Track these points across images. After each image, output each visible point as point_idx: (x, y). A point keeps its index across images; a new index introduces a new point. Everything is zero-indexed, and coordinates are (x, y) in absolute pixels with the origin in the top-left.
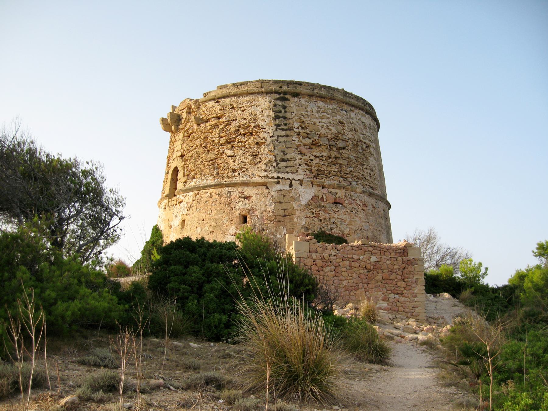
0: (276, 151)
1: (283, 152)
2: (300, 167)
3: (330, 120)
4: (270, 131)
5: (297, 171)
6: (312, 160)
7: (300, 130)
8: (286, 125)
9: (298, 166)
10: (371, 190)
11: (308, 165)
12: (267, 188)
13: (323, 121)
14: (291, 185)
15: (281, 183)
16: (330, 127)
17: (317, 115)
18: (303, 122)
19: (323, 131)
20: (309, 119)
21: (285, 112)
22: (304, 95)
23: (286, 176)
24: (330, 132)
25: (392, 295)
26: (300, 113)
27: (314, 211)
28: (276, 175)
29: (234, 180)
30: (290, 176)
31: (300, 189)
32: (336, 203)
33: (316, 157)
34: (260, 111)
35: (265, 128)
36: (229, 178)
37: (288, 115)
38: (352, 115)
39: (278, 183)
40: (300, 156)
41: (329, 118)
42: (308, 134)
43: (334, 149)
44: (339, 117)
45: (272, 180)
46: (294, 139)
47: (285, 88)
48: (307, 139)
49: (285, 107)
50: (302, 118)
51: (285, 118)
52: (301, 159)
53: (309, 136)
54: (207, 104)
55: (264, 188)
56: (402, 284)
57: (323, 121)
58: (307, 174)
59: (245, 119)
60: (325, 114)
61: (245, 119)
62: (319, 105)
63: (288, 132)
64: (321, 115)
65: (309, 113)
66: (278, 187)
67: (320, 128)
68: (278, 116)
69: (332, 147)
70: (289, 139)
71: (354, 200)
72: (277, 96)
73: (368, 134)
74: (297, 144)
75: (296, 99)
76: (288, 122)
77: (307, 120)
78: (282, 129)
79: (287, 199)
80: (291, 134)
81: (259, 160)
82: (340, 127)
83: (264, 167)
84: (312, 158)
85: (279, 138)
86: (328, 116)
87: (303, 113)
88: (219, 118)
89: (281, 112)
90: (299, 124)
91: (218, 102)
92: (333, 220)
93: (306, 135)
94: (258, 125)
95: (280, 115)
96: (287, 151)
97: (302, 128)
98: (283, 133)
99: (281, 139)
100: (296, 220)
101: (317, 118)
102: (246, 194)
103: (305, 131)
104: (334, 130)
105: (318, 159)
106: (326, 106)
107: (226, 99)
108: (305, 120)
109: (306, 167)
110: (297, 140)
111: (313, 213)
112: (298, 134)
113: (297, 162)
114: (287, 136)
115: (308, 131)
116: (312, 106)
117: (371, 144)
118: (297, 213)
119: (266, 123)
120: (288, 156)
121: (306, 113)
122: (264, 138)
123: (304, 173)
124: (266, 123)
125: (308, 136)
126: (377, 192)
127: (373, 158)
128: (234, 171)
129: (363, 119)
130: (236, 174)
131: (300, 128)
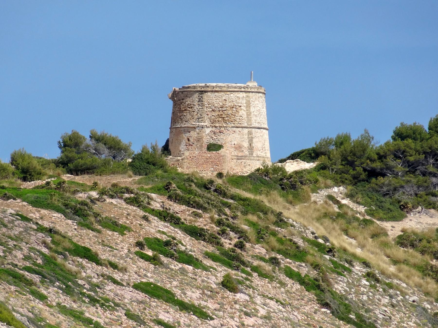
7: (207, 105)
8: (202, 104)
10: (239, 125)
17: (214, 99)
19: (216, 105)
23: (201, 124)
28: (198, 124)
29: (185, 125)
30: (202, 124)
31: (206, 129)
36: (184, 124)
37: (203, 100)
38: (232, 95)
47: (203, 89)
49: (202, 97)
51: (202, 101)
56: (218, 163)
70: (203, 109)
75: (207, 93)
77: (210, 101)
82: (224, 102)
98: (201, 107)
99: (200, 110)
104: (221, 104)
112: (207, 107)
115: (210, 105)
118: (204, 137)
129: (238, 96)
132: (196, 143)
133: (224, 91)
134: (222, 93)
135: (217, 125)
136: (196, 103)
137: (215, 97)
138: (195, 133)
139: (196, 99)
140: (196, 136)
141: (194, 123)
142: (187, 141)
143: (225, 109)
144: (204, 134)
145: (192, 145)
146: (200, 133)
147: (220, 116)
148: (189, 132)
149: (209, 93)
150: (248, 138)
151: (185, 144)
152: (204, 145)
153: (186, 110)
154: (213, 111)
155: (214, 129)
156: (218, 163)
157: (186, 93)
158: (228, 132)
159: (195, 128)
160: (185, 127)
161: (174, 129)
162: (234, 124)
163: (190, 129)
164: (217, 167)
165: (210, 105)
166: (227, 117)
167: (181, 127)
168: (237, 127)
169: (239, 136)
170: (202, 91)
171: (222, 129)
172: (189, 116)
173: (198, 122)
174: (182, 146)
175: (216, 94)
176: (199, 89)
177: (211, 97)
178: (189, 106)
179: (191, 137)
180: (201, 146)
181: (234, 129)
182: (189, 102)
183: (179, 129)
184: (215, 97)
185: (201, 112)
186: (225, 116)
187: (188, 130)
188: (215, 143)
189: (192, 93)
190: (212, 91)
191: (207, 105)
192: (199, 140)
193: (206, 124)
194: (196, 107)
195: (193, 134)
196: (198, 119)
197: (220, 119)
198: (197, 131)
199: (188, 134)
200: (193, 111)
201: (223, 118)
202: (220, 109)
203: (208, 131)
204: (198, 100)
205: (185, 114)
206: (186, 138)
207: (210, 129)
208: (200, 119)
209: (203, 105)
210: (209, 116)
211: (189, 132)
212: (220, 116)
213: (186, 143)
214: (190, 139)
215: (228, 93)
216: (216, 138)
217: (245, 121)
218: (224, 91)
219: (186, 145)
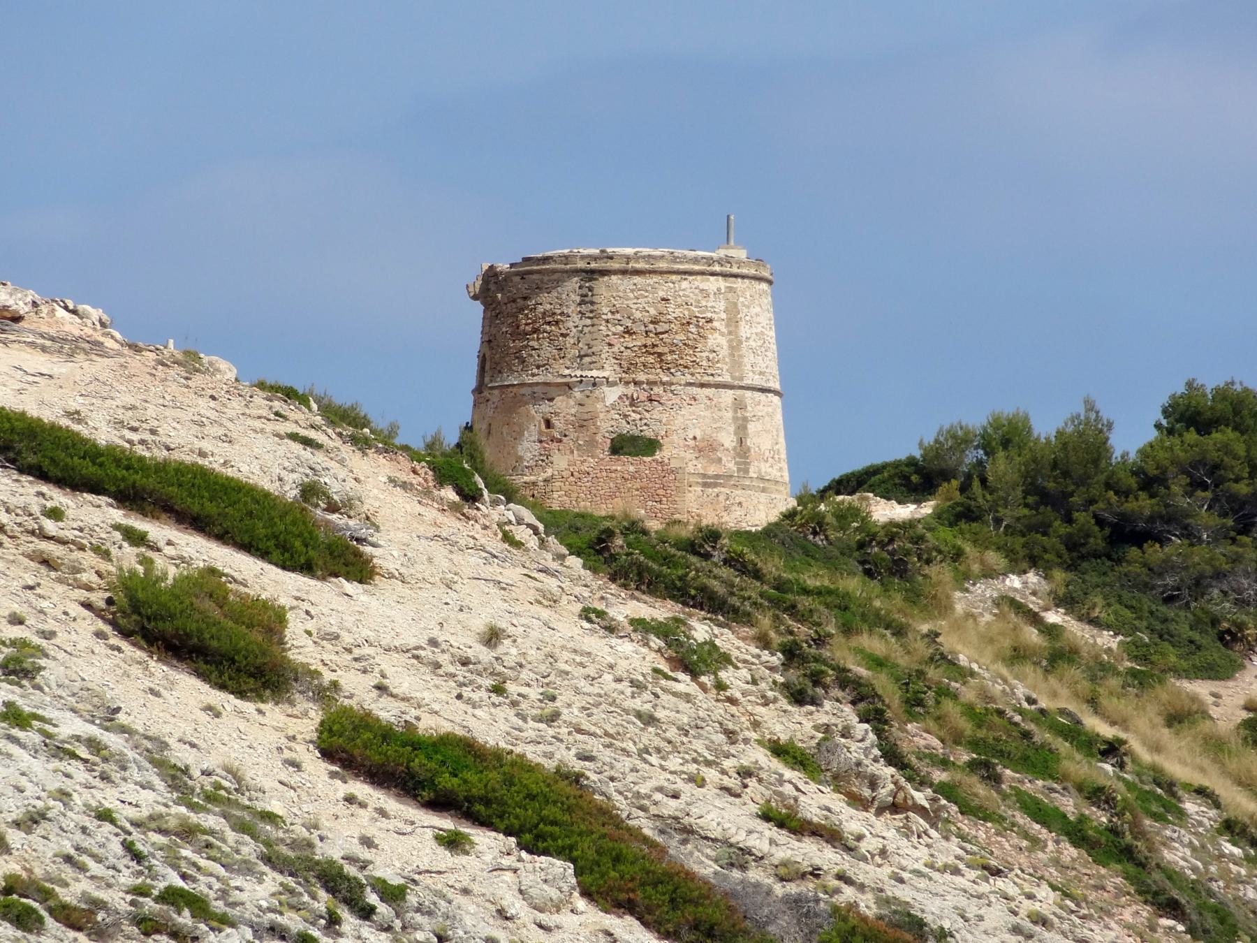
7: (610, 316)
8: (592, 311)
10: (706, 379)
12: (570, 388)
17: (631, 295)
19: (638, 315)
22: (615, 272)
23: (589, 374)
25: (650, 503)
28: (579, 373)
29: (536, 379)
30: (595, 373)
36: (533, 375)
37: (596, 299)
38: (685, 284)
40: (606, 348)
44: (661, 294)
47: (593, 265)
49: (590, 289)
51: (592, 303)
56: (661, 492)
65: (621, 294)
66: (582, 387)
73: (709, 304)
75: (606, 278)
76: (595, 307)
82: (661, 306)
88: (525, 298)
89: (586, 296)
97: (613, 313)
98: (589, 322)
104: (653, 312)
112: (607, 321)
117: (714, 315)
118: (601, 416)
120: (593, 350)
126: (720, 379)
127: (717, 335)
133: (662, 273)
134: (656, 278)
135: (641, 377)
136: (572, 309)
137: (632, 291)
138: (572, 402)
139: (573, 296)
140: (573, 411)
141: (567, 372)
142: (543, 427)
143: (666, 327)
144: (599, 406)
145: (560, 441)
147: (648, 349)
148: (551, 400)
149: (614, 278)
150: (735, 419)
152: (599, 438)
153: (536, 331)
154: (628, 332)
156: (661, 492)
158: (676, 400)
159: (569, 386)
160: (537, 384)
161: (496, 392)
162: (692, 375)
163: (552, 391)
164: (659, 506)
165: (618, 316)
166: (672, 352)
167: (522, 385)
168: (702, 385)
169: (708, 413)
170: (593, 272)
171: (658, 390)
172: (547, 350)
173: (581, 367)
174: (526, 444)
175: (637, 279)
176: (581, 265)
177: (622, 288)
178: (548, 319)
179: (557, 414)
180: (592, 443)
181: (695, 390)
183: (515, 390)
184: (632, 291)
186: (666, 350)
187: (547, 392)
188: (637, 433)
189: (556, 276)
190: (624, 272)
191: (610, 316)
192: (583, 423)
193: (606, 374)
194: (574, 322)
195: (565, 406)
197: (651, 359)
199: (545, 407)
200: (562, 335)
201: (660, 355)
202: (651, 327)
203: (612, 395)
204: (578, 299)
205: (534, 344)
206: (539, 417)
207: (619, 390)
208: (587, 360)
209: (595, 315)
210: (615, 349)
211: (551, 400)
212: (648, 349)
213: (540, 433)
214: (554, 421)
215: (674, 277)
216: (638, 416)
217: (726, 367)
218: (662, 273)
219: (541, 442)
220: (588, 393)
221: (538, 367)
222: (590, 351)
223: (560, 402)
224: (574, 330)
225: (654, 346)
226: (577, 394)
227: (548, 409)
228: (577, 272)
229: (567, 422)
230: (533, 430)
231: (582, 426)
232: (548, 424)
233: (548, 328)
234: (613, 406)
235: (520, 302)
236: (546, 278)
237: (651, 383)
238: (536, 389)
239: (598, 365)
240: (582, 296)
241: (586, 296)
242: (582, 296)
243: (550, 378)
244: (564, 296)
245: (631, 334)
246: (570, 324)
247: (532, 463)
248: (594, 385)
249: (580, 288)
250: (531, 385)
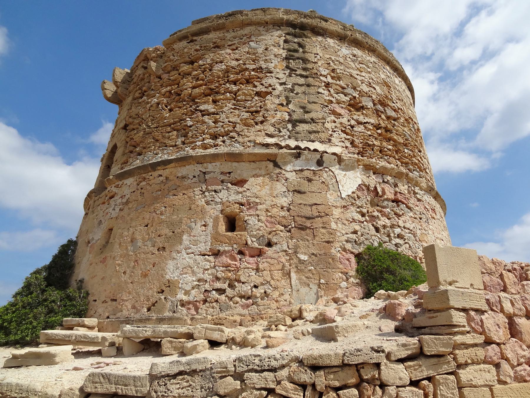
0: (290, 106)
1: (303, 108)
2: (335, 135)
3: (373, 77)
4: (281, 76)
5: (330, 140)
6: (352, 127)
7: (329, 79)
8: (305, 69)
9: (330, 132)
11: (347, 134)
12: (276, 165)
13: (363, 74)
14: (320, 163)
15: (303, 157)
16: (374, 86)
18: (333, 70)
19: (365, 88)
20: (342, 68)
21: (304, 52)
22: (332, 35)
23: (312, 146)
24: (374, 91)
26: (328, 56)
27: (365, 211)
28: (293, 143)
29: (212, 151)
32: (396, 201)
33: (359, 123)
34: (263, 47)
35: (271, 72)
39: (298, 156)
41: (370, 73)
42: (343, 88)
43: (383, 116)
45: (285, 150)
46: (321, 90)
48: (342, 96)
50: (332, 64)
51: (305, 61)
52: (335, 122)
53: (345, 91)
54: (175, 46)
55: (271, 165)
57: (363, 74)
58: (347, 147)
59: (237, 60)
60: (364, 66)
61: (237, 60)
62: (355, 52)
63: (310, 80)
64: (358, 66)
65: (342, 60)
66: (298, 164)
67: (360, 82)
68: (293, 56)
69: (380, 114)
70: (312, 90)
71: (419, 200)
72: (291, 30)
74: (328, 98)
75: (320, 38)
76: (309, 66)
77: (340, 69)
78: (302, 76)
79: (315, 186)
80: (317, 84)
81: (261, 119)
83: (271, 130)
84: (353, 122)
85: (296, 87)
86: (369, 70)
87: (333, 58)
88: (192, 63)
89: (296, 51)
90: (327, 71)
91: (192, 41)
92: (398, 231)
93: (340, 89)
94: (261, 68)
95: (296, 55)
96: (310, 107)
97: (333, 78)
98: (302, 81)
99: (297, 89)
100: (333, 226)
101: (353, 68)
102: (235, 176)
103: (338, 82)
105: (362, 127)
106: (364, 56)
107: (205, 36)
108: (336, 67)
109: (343, 135)
110: (326, 92)
111: (363, 215)
112: (327, 85)
113: (328, 125)
114: (308, 86)
116: (345, 51)
118: (336, 213)
119: (273, 65)
120: (313, 115)
121: (337, 59)
122: (270, 85)
123: (342, 144)
124: (273, 65)
125: (342, 90)
128: (215, 137)
130: (219, 141)
131: (329, 76)
132: (283, 241)
136: (276, 65)
138: (280, 187)
140: (284, 201)
142: (222, 227)
144: (331, 197)
145: (260, 253)
146: (305, 186)
148: (241, 183)
149: (331, 41)
151: (204, 247)
153: (212, 92)
155: (373, 180)
157: (212, 36)
160: (215, 157)
161: (130, 181)
163: (241, 170)
170: (303, 27)
175: (358, 52)
178: (232, 77)
179: (250, 205)
180: (324, 260)
182: (234, 63)
183: (166, 172)
185: (304, 100)
187: (234, 169)
189: (247, 30)
190: (342, 38)
191: (329, 79)
192: (304, 223)
193: (338, 150)
194: (278, 77)
195: (268, 195)
196: (295, 123)
198: (292, 176)
199: (229, 195)
200: (258, 94)
202: (379, 107)
203: (350, 181)
204: (284, 53)
205: (210, 108)
206: (214, 211)
208: (302, 127)
209: (310, 75)
213: (216, 238)
214: (247, 215)
216: (388, 223)
219: (217, 254)
220: (307, 174)
221: (215, 137)
222: (307, 116)
223: (258, 187)
224: (280, 88)
225: (387, 130)
226: (290, 171)
227: (233, 197)
228: (278, 24)
229: (273, 220)
230: (200, 236)
231: (303, 228)
232: (232, 224)
233: (234, 88)
234: (353, 198)
235: (186, 68)
236: (229, 35)
237: (399, 176)
238: (210, 167)
239: (323, 136)
240: (289, 50)
241: (296, 51)
242: (289, 50)
243: (237, 148)
244: (260, 51)
245: (358, 110)
246: (272, 81)
247: (196, 295)
248: (320, 163)
249: (286, 41)
250: (200, 160)
